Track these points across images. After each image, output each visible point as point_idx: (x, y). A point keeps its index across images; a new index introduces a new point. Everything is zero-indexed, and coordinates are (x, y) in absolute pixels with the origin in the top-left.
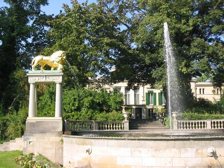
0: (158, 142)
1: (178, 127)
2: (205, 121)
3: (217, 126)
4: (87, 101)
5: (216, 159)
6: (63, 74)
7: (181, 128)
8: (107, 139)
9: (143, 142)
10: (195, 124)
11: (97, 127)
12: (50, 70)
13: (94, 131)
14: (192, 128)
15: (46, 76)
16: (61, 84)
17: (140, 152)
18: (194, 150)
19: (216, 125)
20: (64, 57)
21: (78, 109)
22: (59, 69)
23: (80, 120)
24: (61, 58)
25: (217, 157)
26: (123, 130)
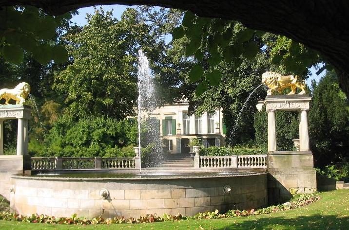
0: (96, 183)
1: (200, 164)
2: (231, 157)
3: (244, 164)
4: (95, 136)
5: (109, 202)
6: (23, 109)
7: (203, 165)
8: (24, 179)
9: (45, 182)
10: (220, 161)
11: (100, 165)
12: (15, 104)
13: (96, 169)
14: (213, 166)
15: (7, 111)
16: (23, 119)
17: (43, 192)
18: (87, 192)
19: (243, 162)
20: (27, 90)
21: (87, 144)
22: (21, 103)
23: (85, 157)
24: (23, 90)
25: (111, 200)
26: (134, 169)
